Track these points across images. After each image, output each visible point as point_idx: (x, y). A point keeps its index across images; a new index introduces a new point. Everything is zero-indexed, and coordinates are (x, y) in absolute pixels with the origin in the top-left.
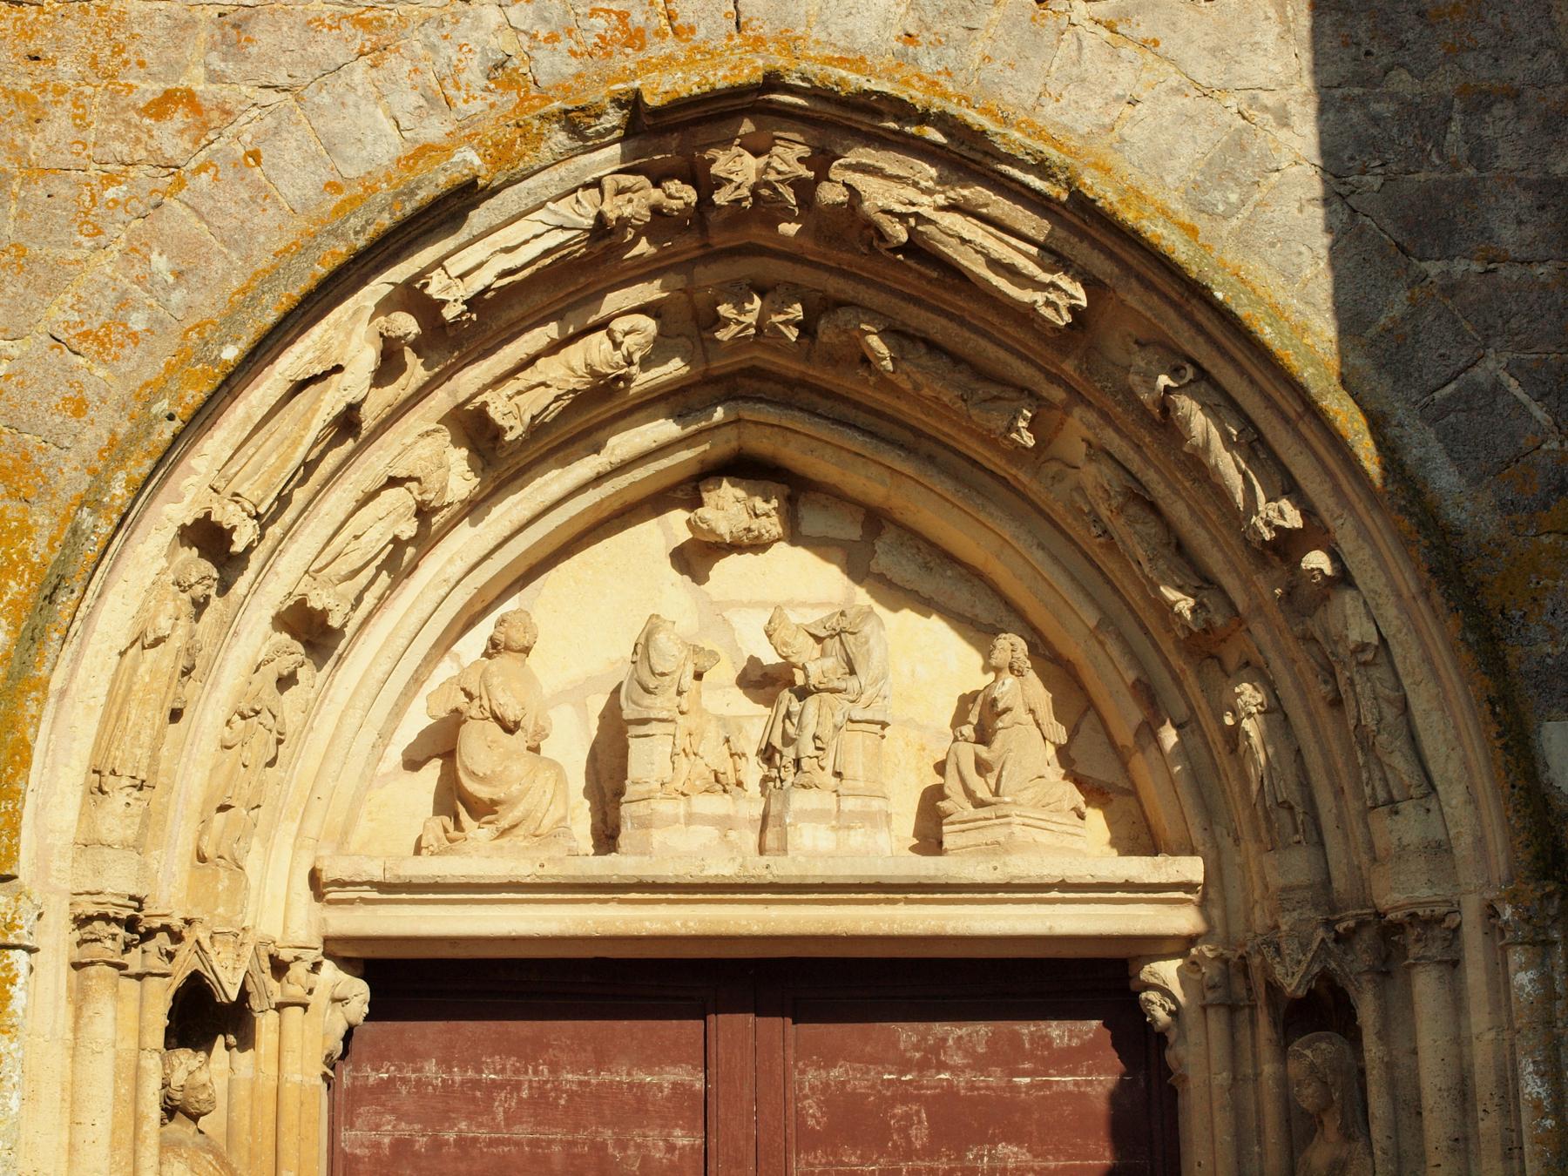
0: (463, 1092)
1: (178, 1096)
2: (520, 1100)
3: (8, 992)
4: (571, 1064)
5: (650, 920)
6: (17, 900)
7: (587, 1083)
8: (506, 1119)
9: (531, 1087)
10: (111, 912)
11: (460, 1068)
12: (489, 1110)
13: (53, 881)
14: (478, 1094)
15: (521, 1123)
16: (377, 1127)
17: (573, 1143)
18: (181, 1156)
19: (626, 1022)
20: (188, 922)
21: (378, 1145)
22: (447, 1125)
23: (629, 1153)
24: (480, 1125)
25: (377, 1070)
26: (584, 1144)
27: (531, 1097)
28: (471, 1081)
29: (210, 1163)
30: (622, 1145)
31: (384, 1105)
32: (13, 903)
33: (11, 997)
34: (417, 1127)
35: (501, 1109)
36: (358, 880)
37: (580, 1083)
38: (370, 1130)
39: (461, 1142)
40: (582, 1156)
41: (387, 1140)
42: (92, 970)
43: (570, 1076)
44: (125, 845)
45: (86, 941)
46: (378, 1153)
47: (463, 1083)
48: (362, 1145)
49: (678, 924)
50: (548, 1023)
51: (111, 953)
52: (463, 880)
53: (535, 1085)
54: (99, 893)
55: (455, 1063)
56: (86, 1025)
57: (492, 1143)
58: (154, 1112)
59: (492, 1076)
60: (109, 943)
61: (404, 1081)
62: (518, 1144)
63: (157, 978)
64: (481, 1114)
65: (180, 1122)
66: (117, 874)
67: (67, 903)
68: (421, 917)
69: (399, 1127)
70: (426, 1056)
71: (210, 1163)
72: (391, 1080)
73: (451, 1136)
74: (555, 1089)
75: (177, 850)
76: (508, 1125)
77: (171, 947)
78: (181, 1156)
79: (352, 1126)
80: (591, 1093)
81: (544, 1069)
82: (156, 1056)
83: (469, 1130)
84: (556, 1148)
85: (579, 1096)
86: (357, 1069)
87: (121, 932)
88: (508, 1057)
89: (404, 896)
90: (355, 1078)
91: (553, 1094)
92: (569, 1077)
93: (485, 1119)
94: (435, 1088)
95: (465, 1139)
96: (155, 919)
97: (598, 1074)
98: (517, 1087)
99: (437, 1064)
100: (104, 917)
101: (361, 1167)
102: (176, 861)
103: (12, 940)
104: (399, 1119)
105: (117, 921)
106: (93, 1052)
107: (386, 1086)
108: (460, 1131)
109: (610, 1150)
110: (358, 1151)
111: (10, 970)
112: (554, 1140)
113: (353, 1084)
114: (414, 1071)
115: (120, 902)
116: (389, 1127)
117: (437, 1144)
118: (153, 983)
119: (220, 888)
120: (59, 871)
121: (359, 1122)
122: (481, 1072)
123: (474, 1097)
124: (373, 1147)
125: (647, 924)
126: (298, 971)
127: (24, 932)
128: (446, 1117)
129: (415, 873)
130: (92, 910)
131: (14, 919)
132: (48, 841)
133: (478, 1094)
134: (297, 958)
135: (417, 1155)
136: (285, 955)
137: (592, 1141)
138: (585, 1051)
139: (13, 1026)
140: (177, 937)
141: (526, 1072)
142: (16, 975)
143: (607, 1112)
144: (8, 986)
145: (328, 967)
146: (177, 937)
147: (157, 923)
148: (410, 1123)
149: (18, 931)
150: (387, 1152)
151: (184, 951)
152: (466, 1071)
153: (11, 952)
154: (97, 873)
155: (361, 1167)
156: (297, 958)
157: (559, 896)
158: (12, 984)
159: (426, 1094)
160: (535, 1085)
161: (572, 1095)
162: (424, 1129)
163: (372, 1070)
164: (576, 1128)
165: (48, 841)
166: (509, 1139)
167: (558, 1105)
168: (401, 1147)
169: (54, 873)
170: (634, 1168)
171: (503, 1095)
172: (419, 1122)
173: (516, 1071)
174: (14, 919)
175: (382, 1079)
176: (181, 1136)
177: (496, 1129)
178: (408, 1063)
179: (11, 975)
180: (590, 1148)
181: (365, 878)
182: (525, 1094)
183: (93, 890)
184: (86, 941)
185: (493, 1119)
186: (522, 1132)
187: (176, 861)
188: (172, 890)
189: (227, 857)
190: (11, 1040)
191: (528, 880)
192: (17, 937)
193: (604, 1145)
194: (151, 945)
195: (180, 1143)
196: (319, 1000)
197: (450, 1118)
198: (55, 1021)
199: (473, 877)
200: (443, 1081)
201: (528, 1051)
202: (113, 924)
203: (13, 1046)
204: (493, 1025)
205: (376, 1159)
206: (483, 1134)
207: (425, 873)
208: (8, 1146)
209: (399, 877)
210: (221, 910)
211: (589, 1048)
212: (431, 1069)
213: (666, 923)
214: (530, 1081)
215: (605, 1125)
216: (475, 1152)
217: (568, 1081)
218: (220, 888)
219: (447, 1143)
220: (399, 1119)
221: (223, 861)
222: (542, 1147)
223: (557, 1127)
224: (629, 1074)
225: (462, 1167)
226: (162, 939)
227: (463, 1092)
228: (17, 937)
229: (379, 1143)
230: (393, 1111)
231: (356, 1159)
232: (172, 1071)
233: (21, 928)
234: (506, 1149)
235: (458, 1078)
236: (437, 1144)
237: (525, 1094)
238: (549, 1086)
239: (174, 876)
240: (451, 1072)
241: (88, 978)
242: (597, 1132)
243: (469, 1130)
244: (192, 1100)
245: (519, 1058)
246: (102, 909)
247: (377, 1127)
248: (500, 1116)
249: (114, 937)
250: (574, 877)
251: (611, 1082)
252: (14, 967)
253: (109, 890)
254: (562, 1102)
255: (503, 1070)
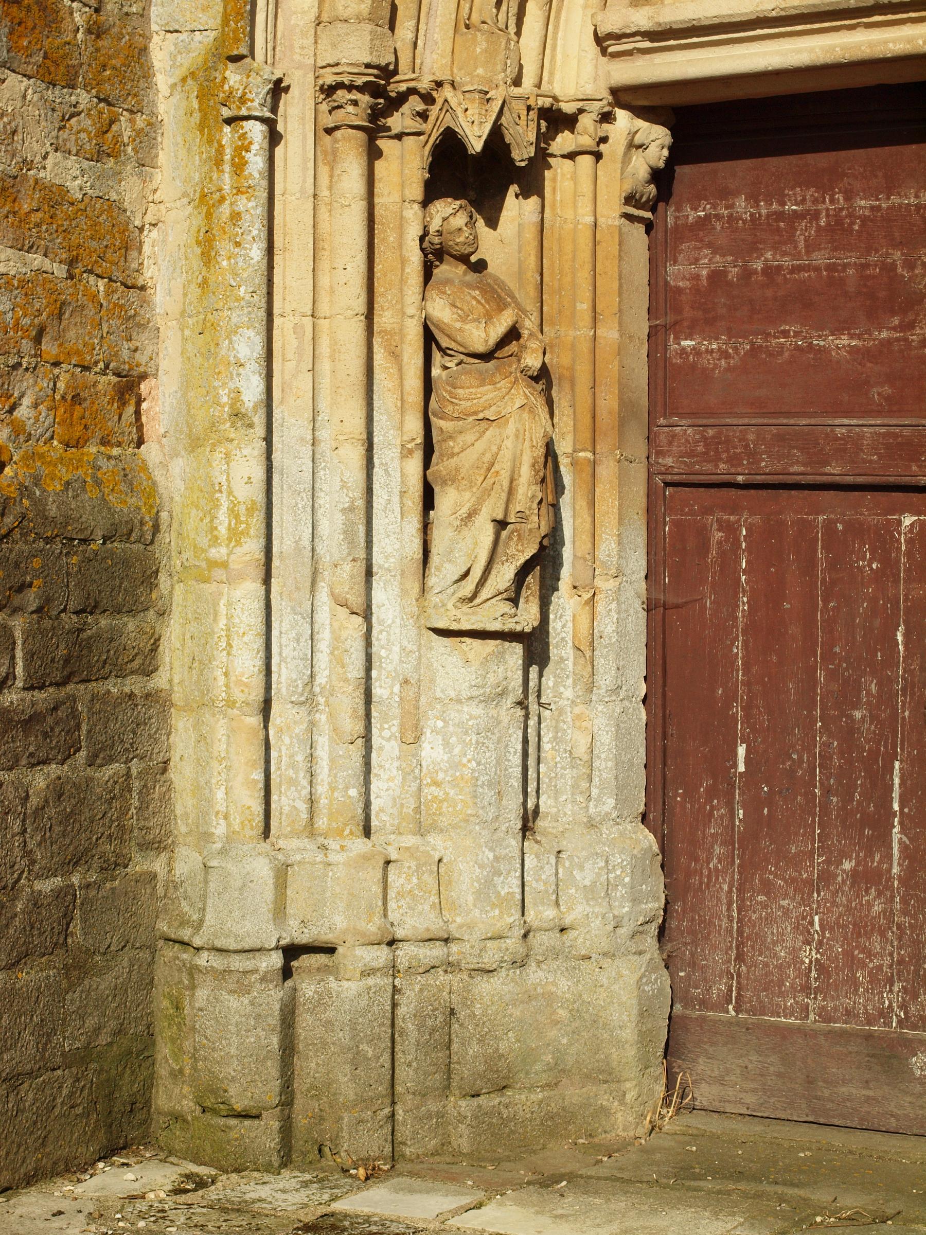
0: (769, 224)
1: (436, 240)
2: (819, 228)
3: (243, 158)
4: (864, 191)
5: (894, 41)
6: (248, 76)
7: (879, 208)
8: (807, 247)
9: (828, 216)
10: (346, 80)
11: (766, 201)
12: (792, 240)
13: (297, 57)
14: (782, 225)
15: (820, 249)
16: (696, 262)
17: (865, 266)
18: (445, 293)
19: (914, 147)
20: (439, 84)
21: (697, 277)
22: (755, 255)
23: (917, 272)
24: (784, 254)
25: (695, 209)
26: (876, 266)
27: (828, 224)
28: (775, 213)
29: (475, 298)
30: (910, 265)
31: (702, 241)
32: (245, 80)
33: (246, 162)
34: (730, 258)
35: (802, 238)
36: (628, 31)
37: (872, 208)
38: (690, 265)
39: (768, 271)
40: (874, 277)
41: (704, 272)
42: (338, 134)
43: (863, 203)
44: (360, 20)
45: (334, 108)
46: (698, 285)
47: (768, 216)
48: (684, 278)
49: (921, 42)
50: (843, 154)
51: (353, 118)
52: (716, 21)
53: (831, 213)
54: (337, 64)
55: (761, 198)
56: (336, 182)
57: (795, 269)
58: (415, 258)
59: (794, 207)
60: (350, 109)
61: (718, 217)
62: (817, 269)
63: (412, 137)
64: (785, 243)
65: (449, 264)
66: (351, 46)
67: (311, 77)
68: (688, 61)
69: (714, 260)
70: (736, 193)
71: (475, 298)
72: (707, 217)
73: (758, 266)
74: (850, 215)
75: (438, 20)
76: (808, 252)
77: (421, 107)
78: (445, 293)
79: (675, 262)
80: (882, 216)
81: (840, 197)
82: (416, 207)
83: (774, 259)
84: (851, 272)
85: (872, 221)
86: (678, 210)
87: (365, 99)
88: (808, 188)
89: (672, 42)
90: (677, 218)
91: (848, 221)
92: (863, 203)
93: (788, 248)
94: (744, 222)
95: (770, 268)
96: (401, 84)
97: (888, 198)
98: (816, 216)
99: (746, 199)
100: (340, 86)
101: (683, 298)
102: (437, 30)
103: (244, 112)
104: (714, 253)
105: (361, 89)
106: (343, 206)
107: (703, 223)
108: (767, 260)
109: (899, 270)
110: (681, 284)
111: (245, 139)
112: (849, 264)
113: (675, 223)
114: (726, 208)
115: (356, 71)
116: (706, 261)
117: (747, 274)
118: (409, 141)
119: (478, 50)
120: (302, 48)
121: (681, 258)
122: (784, 204)
123: (778, 229)
124: (693, 279)
125: (891, 45)
126: (586, 122)
127: (256, 104)
128: (754, 249)
129: (673, 19)
130: (329, 79)
131: (244, 94)
132: (292, 22)
133: (782, 225)
134: (581, 111)
135: (730, 284)
136: (568, 108)
137: (883, 262)
138: (876, 176)
139: (249, 187)
140: (428, 99)
141: (824, 202)
142: (251, 143)
143: (897, 234)
144: (243, 153)
145: (622, 116)
146: (428, 99)
147: (403, 87)
148: (723, 255)
149: (249, 104)
150: (705, 282)
151: (434, 111)
152: (771, 204)
153: (244, 123)
154: (334, 46)
155: (683, 298)
156: (581, 111)
157: (808, 27)
158: (248, 151)
159: (737, 228)
160: (831, 213)
161: (864, 220)
162: (735, 261)
163: (691, 209)
164: (868, 250)
165: (292, 22)
166: (809, 265)
167: (852, 230)
168: (717, 277)
169: (298, 50)
170: (921, 287)
171: (804, 224)
172: (731, 255)
173: (815, 201)
174: (244, 94)
175: (699, 217)
176: (451, 275)
177: (797, 256)
178: (721, 200)
179: (246, 143)
180: (881, 269)
181: (634, 30)
182: (823, 223)
183: (331, 62)
184: (334, 108)
185: (796, 247)
186: (820, 258)
187: (437, 30)
188: (435, 56)
189: (489, 21)
190: (249, 200)
191: (774, 14)
192: (248, 109)
193: (893, 266)
194: (406, 108)
195: (447, 282)
196: (614, 148)
197: (758, 249)
198: (304, 181)
199: (724, 16)
200: (752, 215)
201: (825, 181)
202: (354, 91)
203: (250, 205)
204: (793, 159)
205: (696, 290)
206: (786, 262)
207: (681, 18)
208: (251, 290)
209: (660, 25)
210: (480, 71)
211: (880, 174)
212: (741, 204)
213: (909, 42)
214: (827, 210)
215: (895, 247)
216: (780, 279)
217: (861, 207)
218: (478, 50)
219: (755, 272)
220: (714, 253)
221: (486, 26)
222: (837, 271)
223: (851, 251)
224: (917, 196)
225: (769, 293)
226: (414, 103)
227: (769, 224)
228: (248, 109)
229: (698, 276)
230: (710, 245)
231: (679, 290)
232: (431, 219)
233: (252, 101)
234: (806, 275)
235: (764, 212)
236: (747, 274)
237: (823, 223)
238: (844, 213)
239: (436, 43)
240: (758, 206)
241: (336, 141)
242: (887, 254)
243: (774, 259)
244: (451, 243)
245: (818, 189)
246: (339, 79)
247: (696, 262)
248: (802, 245)
249: (355, 103)
250: (814, 6)
251: (900, 205)
252: (248, 135)
253: (344, 60)
254: (856, 227)
255: (804, 200)
